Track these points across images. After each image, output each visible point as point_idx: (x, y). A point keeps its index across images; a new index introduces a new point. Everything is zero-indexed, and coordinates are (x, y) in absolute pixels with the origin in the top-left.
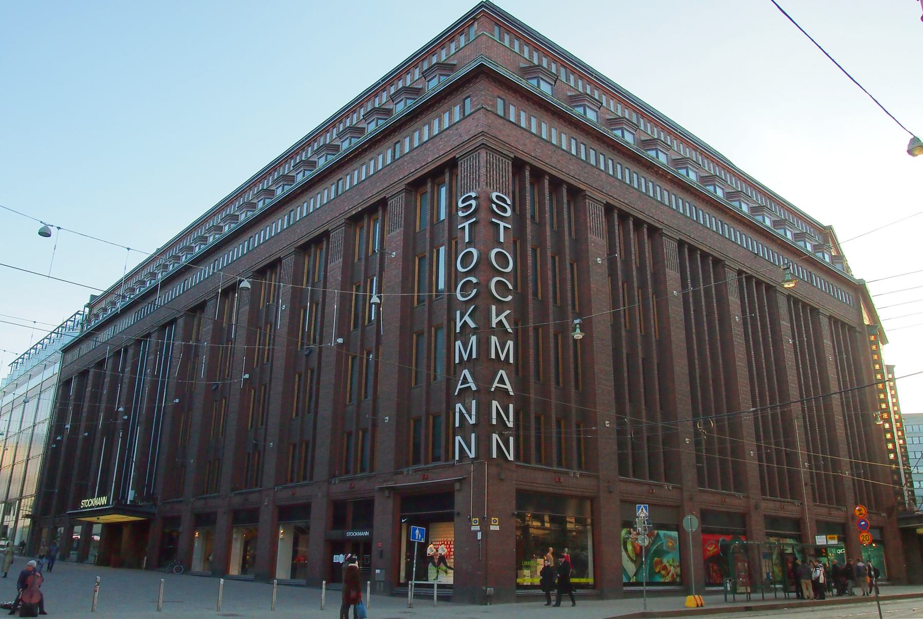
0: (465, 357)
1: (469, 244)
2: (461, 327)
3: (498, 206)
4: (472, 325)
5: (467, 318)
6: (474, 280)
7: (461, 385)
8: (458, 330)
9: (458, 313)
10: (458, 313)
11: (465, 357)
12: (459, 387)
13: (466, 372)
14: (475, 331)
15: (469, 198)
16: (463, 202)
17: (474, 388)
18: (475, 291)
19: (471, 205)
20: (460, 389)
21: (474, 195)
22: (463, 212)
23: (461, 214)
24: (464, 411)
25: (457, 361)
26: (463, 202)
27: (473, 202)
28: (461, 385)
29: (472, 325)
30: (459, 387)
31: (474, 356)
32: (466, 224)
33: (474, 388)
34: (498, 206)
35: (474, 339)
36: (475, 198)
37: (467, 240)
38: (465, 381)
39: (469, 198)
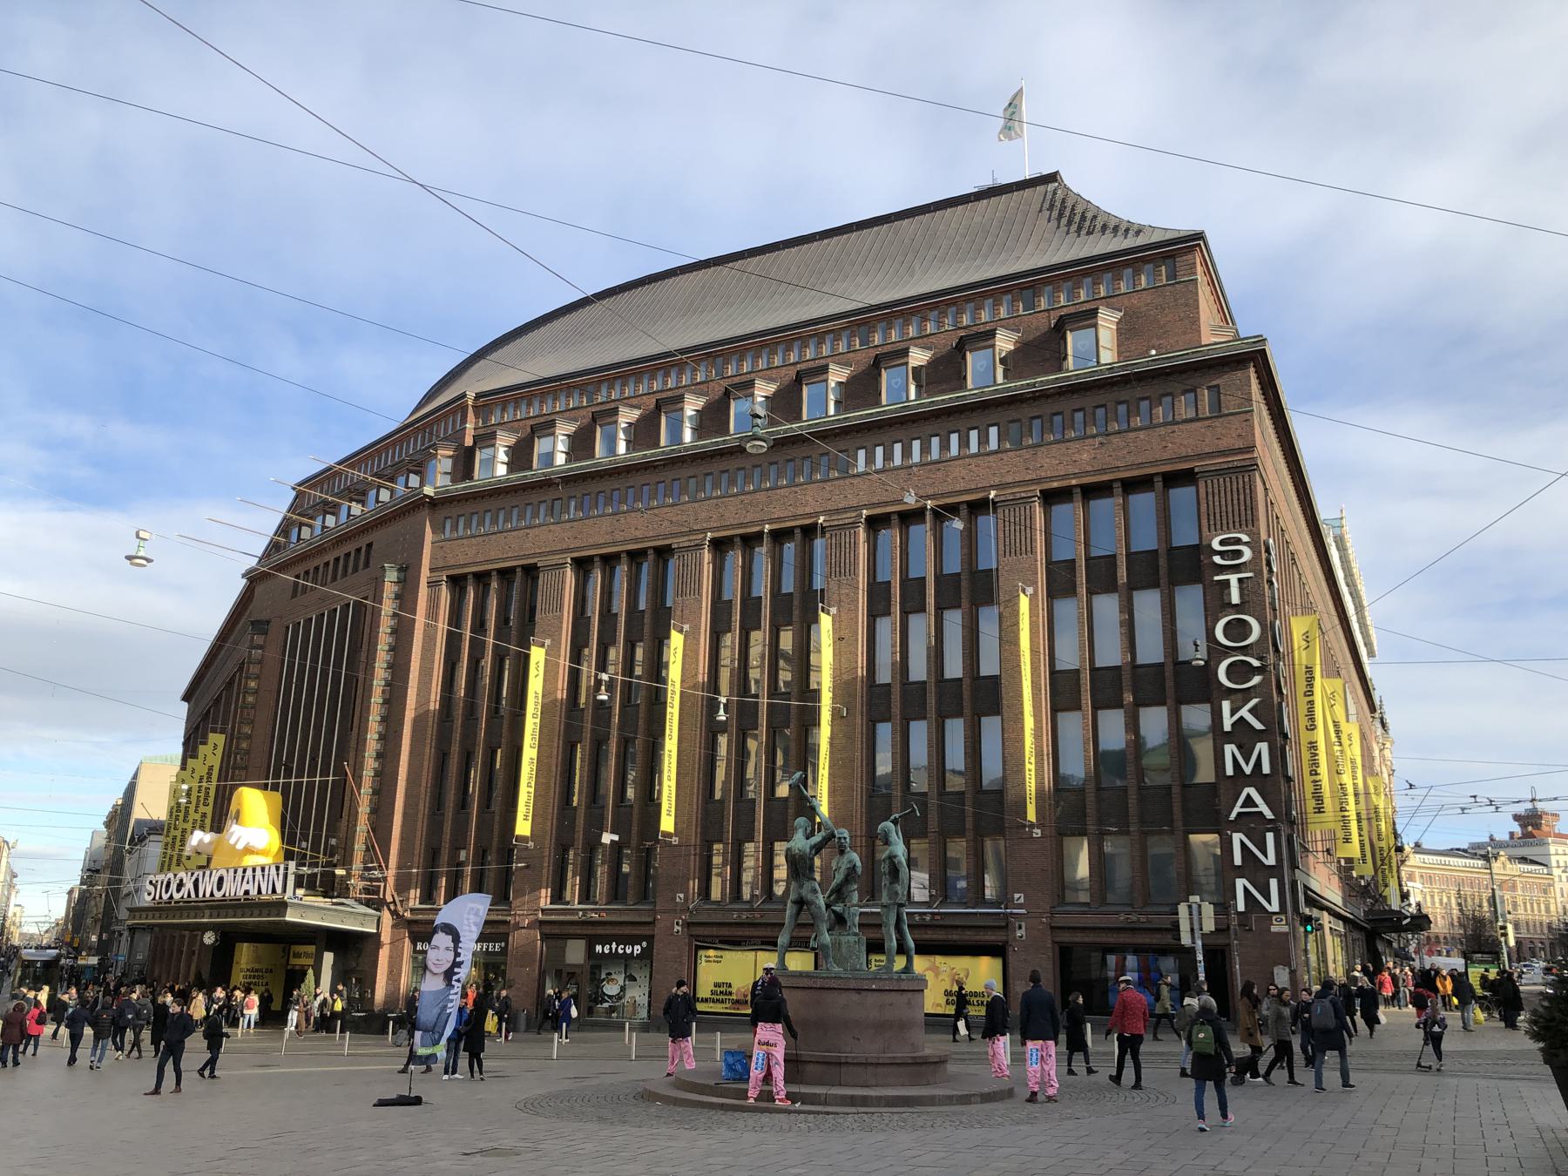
0: (1248, 770)
2: (1233, 725)
4: (1258, 726)
6: (1256, 663)
7: (1241, 807)
8: (1227, 727)
11: (1248, 770)
12: (1237, 809)
13: (1252, 791)
16: (1222, 543)
17: (1269, 814)
19: (1239, 554)
20: (1239, 814)
21: (1245, 538)
22: (1223, 558)
26: (1222, 543)
27: (1247, 554)
28: (1241, 807)
29: (1258, 726)
30: (1237, 809)
31: (1266, 769)
32: (1233, 579)
33: (1269, 814)
35: (1263, 747)
36: (1246, 544)
37: (1235, 599)
38: (1249, 801)
39: (1238, 541)
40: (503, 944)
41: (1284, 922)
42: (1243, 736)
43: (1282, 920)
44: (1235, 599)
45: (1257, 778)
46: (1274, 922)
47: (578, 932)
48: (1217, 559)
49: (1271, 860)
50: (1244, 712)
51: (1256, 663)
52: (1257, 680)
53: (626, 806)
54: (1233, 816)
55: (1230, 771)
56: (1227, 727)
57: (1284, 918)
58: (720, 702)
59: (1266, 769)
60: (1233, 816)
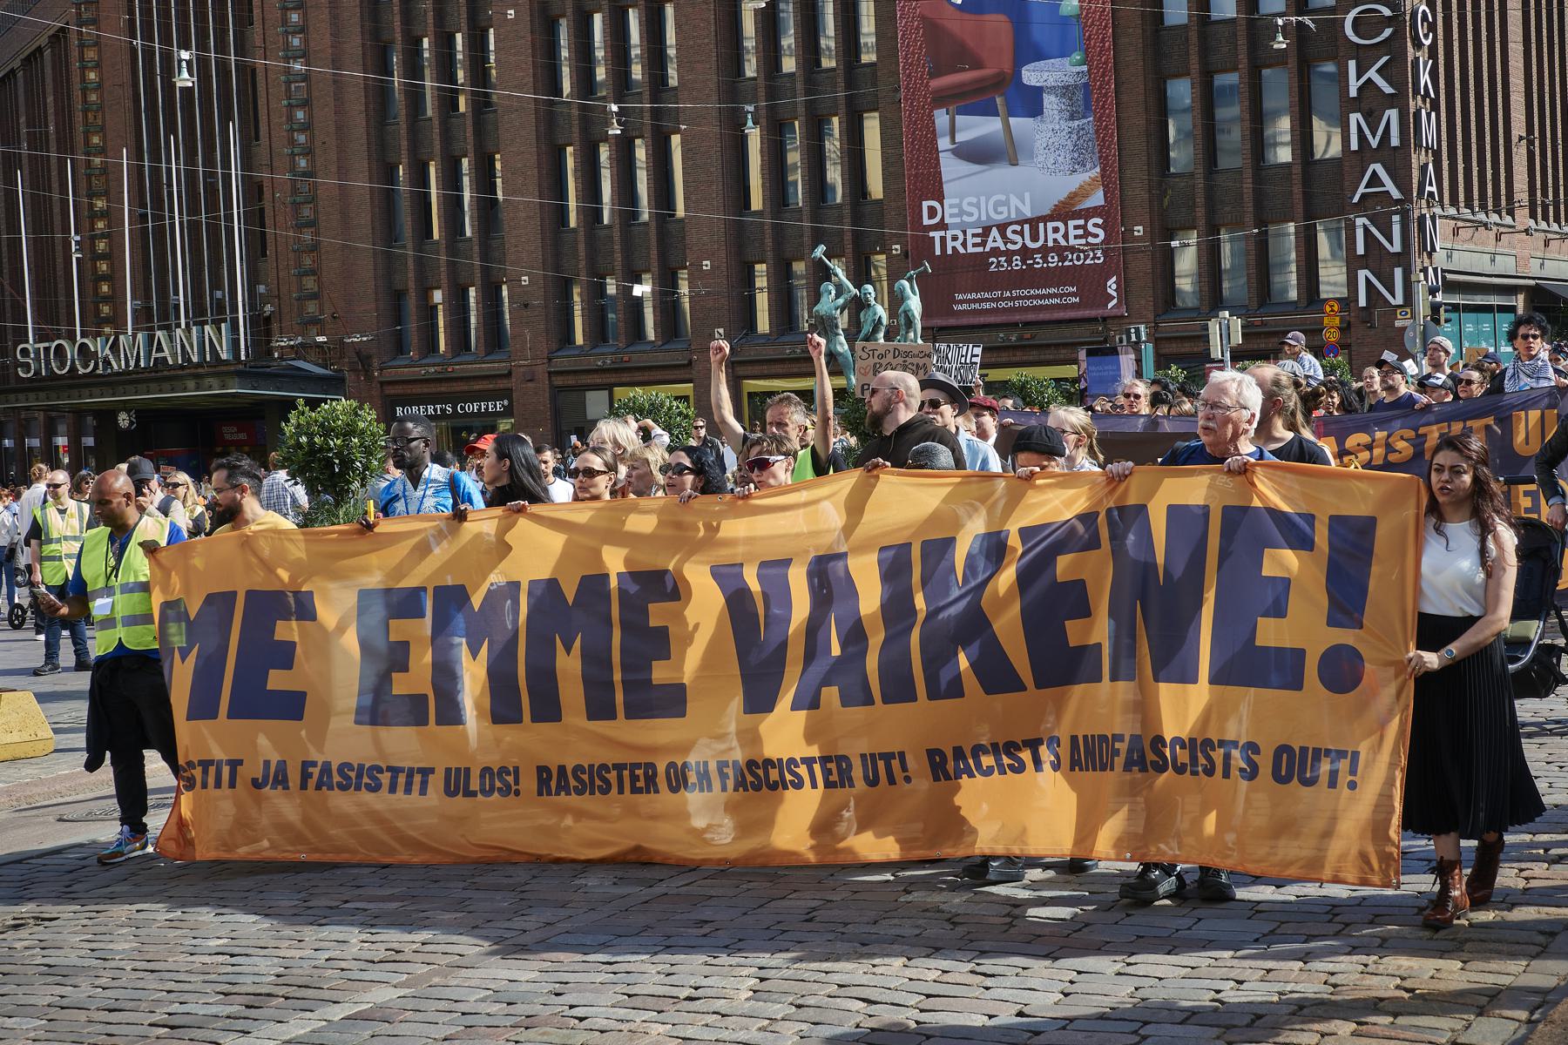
0: (1374, 143)
2: (1360, 90)
4: (1388, 90)
7: (1366, 187)
8: (1353, 93)
9: (1352, 64)
11: (1374, 143)
13: (1378, 168)
14: (1391, 101)
18: (1388, 32)
20: (1363, 195)
28: (1366, 187)
29: (1388, 90)
30: (1361, 190)
31: (1395, 141)
35: (1392, 114)
38: (1375, 180)
40: (506, 402)
41: (1409, 316)
43: (1407, 313)
46: (1399, 317)
47: (599, 381)
49: (1397, 247)
50: (1372, 74)
51: (1387, 12)
52: (1388, 32)
53: (640, 224)
54: (1356, 200)
55: (1354, 146)
56: (1353, 93)
57: (1409, 311)
59: (1395, 141)
60: (1356, 200)
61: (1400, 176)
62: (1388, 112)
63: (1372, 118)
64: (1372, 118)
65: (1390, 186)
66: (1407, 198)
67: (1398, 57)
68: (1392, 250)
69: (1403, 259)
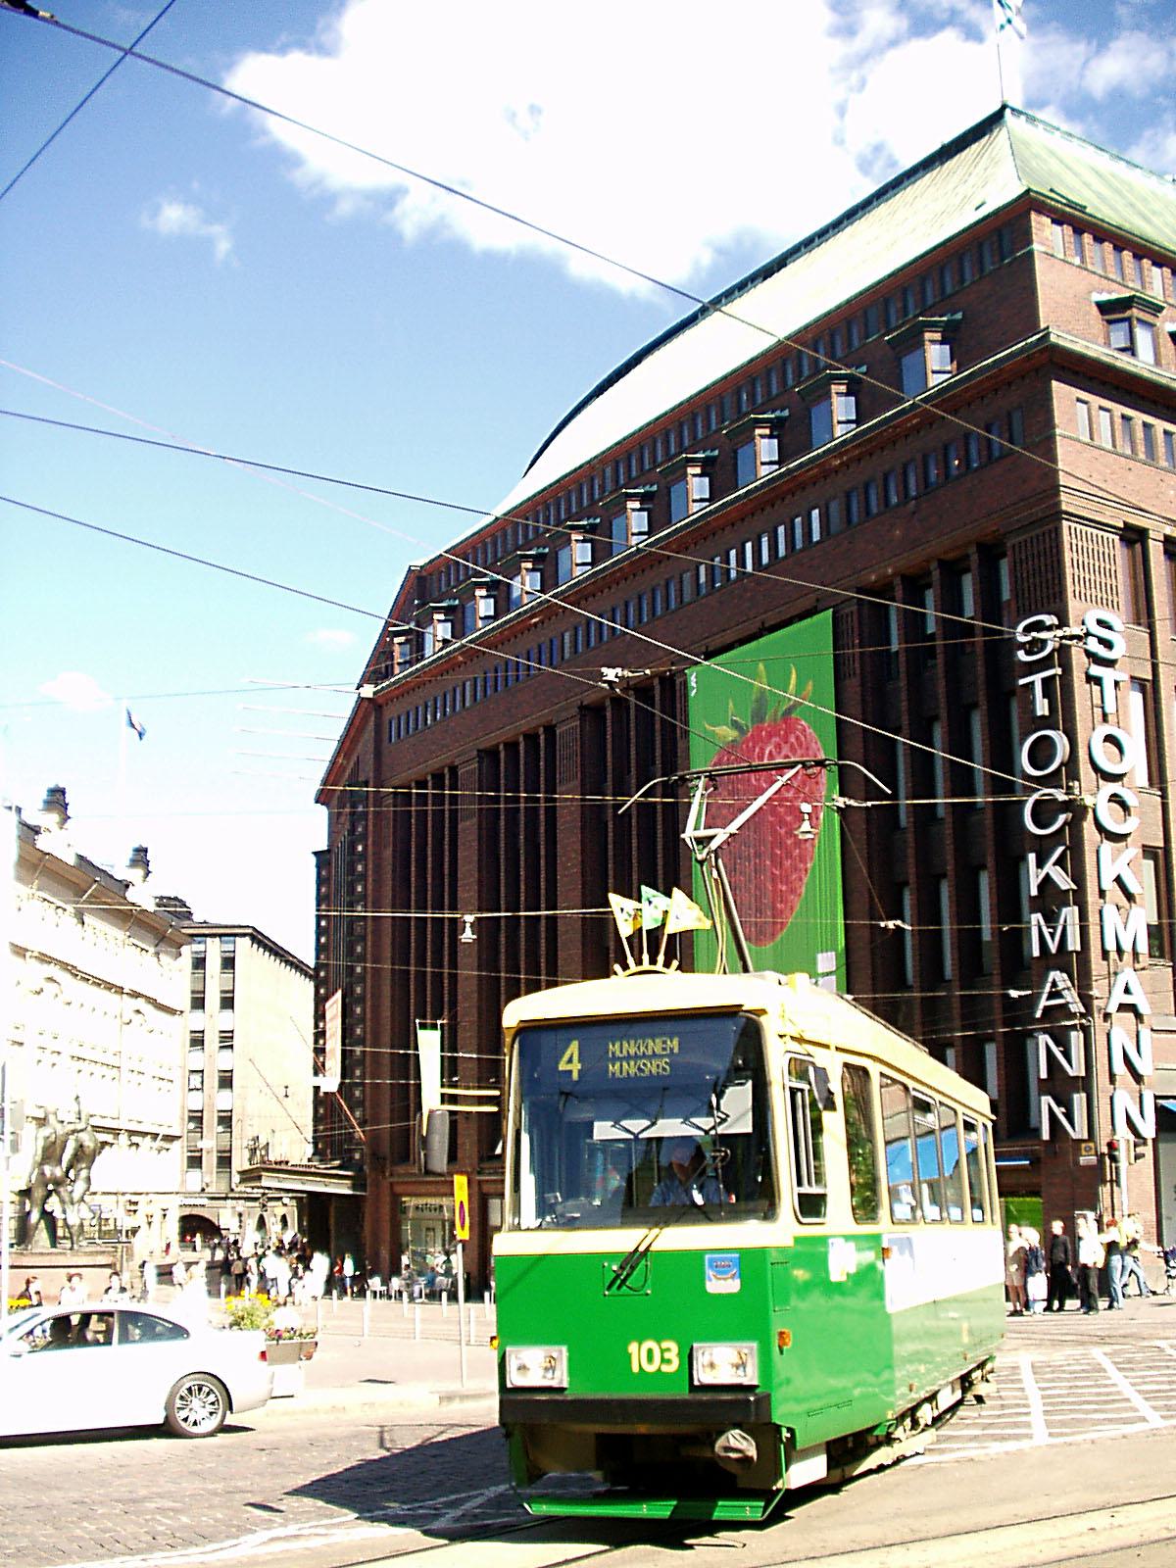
0: (1053, 947)
1: (1048, 722)
2: (1040, 887)
3: (1102, 641)
5: (1051, 869)
6: (1061, 796)
7: (1048, 999)
8: (1034, 892)
9: (1032, 857)
10: (1032, 857)
11: (1053, 947)
13: (1055, 975)
15: (1039, 626)
16: (1027, 630)
17: (1074, 1008)
20: (1046, 1009)
22: (1028, 653)
23: (1022, 655)
24: (1056, 1051)
25: (1036, 953)
26: (1027, 630)
28: (1048, 999)
29: (1064, 881)
30: (1043, 1003)
31: (1073, 944)
32: (1037, 679)
34: (1102, 641)
38: (1055, 994)
41: (1093, 1152)
42: (1050, 900)
44: (1042, 707)
45: (1060, 959)
46: (1084, 1153)
48: (1022, 655)
50: (1051, 869)
52: (1062, 818)
58: (465, 922)
60: (1038, 1015)
61: (1083, 984)
62: (1065, 910)
63: (1051, 918)
64: (1051, 918)
65: (1071, 997)
66: (1089, 1011)
67: (1076, 848)
68: (1072, 1073)
69: (1085, 1083)
